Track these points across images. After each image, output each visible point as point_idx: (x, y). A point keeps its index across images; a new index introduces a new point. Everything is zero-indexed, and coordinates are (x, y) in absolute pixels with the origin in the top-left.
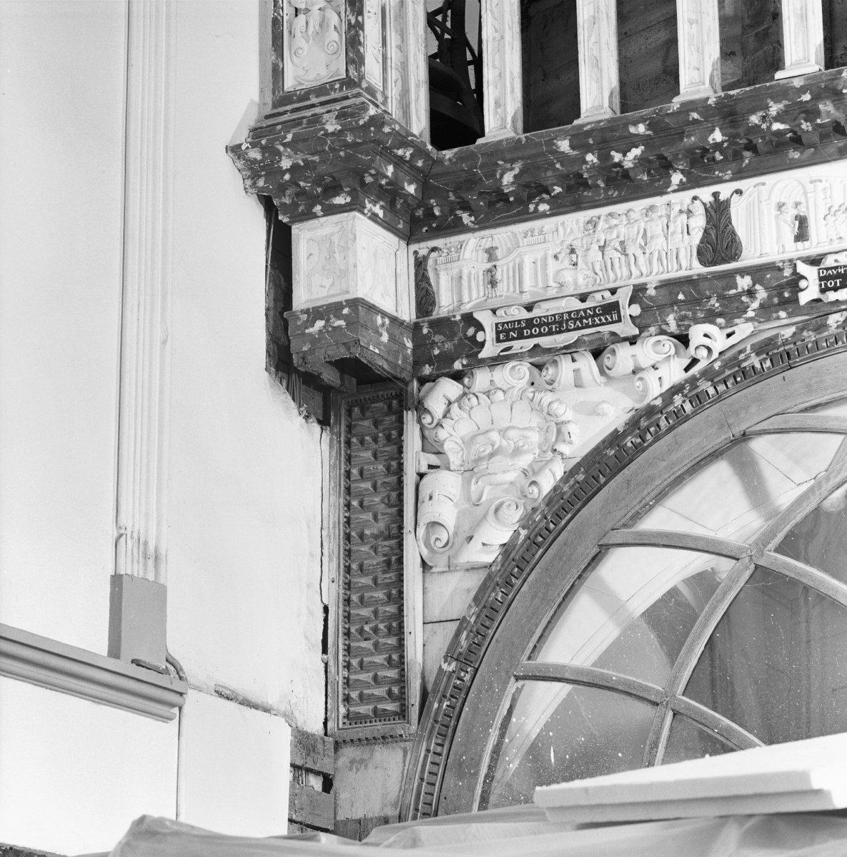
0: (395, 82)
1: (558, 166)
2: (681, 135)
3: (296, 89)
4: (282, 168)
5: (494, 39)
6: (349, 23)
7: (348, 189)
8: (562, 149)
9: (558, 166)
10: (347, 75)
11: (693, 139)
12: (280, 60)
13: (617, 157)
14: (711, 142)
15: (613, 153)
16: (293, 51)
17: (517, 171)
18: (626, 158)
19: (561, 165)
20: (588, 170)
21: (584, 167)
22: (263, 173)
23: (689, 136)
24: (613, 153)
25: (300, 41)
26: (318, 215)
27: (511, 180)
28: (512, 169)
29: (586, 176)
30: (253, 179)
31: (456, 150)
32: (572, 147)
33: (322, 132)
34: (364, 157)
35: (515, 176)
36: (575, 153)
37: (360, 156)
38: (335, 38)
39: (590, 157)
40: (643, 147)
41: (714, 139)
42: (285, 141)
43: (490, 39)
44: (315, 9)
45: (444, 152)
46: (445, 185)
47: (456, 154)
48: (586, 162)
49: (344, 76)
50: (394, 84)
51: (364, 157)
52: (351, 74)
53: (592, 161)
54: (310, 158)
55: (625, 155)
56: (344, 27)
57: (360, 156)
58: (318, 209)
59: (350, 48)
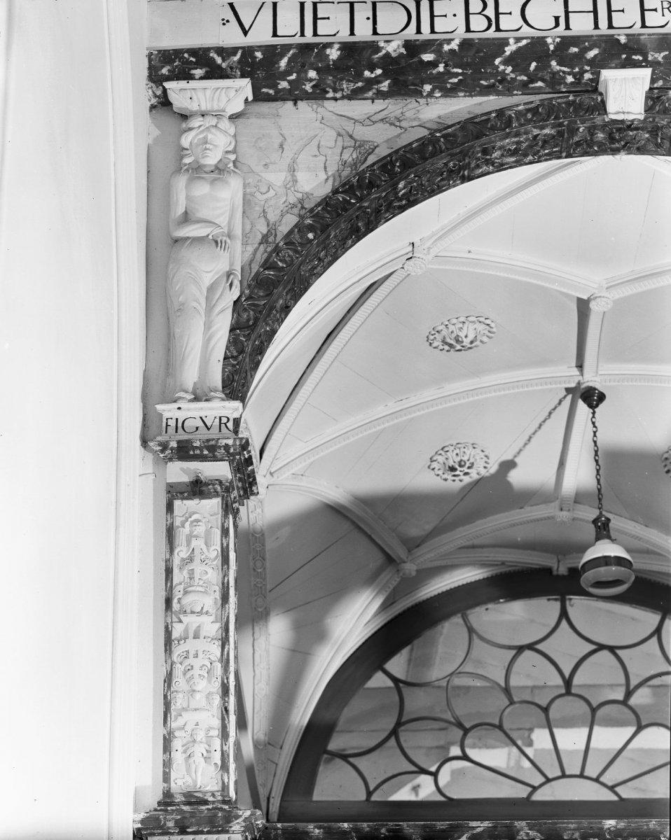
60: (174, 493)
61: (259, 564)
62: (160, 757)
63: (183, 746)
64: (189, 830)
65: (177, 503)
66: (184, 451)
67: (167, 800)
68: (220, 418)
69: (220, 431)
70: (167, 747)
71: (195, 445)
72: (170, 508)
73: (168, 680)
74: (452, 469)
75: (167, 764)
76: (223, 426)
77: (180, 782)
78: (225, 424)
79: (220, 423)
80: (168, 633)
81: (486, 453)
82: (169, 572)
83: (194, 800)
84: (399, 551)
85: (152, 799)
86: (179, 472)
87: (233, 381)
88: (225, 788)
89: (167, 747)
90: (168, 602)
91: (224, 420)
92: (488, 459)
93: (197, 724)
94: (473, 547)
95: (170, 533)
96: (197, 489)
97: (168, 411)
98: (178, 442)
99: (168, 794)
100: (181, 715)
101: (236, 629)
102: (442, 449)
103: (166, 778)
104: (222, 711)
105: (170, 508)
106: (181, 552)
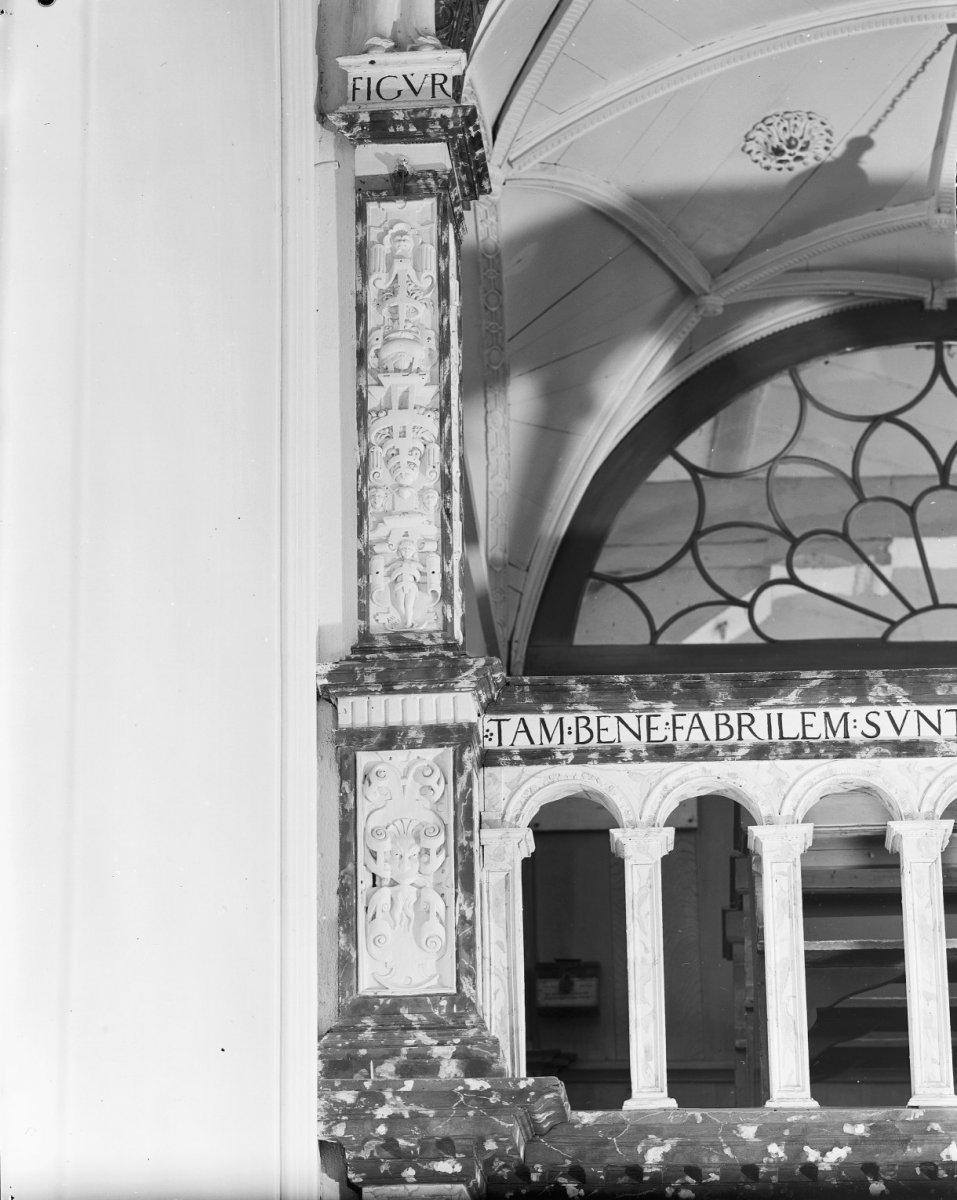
0: (495, 994)
1: (727, 1151)
2: (905, 1142)
3: (379, 994)
4: (375, 1116)
5: (643, 961)
6: (463, 917)
7: (462, 1156)
8: (743, 1136)
9: (727, 1151)
10: (458, 990)
11: (919, 1150)
12: (353, 949)
13: (812, 1155)
14: (945, 1159)
15: (806, 1148)
16: (372, 937)
17: (667, 1148)
18: (825, 1159)
19: (733, 1152)
20: (768, 1165)
21: (765, 1160)
22: (344, 1118)
23: (915, 1145)
24: (806, 1148)
25: (382, 925)
26: (408, 1180)
27: (659, 1159)
28: (661, 1145)
29: (763, 1169)
30: (327, 1122)
31: (599, 1113)
32: (757, 1135)
33: (461, 1088)
34: (502, 1123)
35: (665, 1155)
36: (757, 1140)
37: (497, 1120)
38: (441, 935)
39: (773, 1148)
40: (850, 1149)
41: (948, 1156)
42: (402, 1090)
43: (639, 961)
44: (406, 883)
45: (580, 1114)
46: (560, 1148)
47: (598, 1119)
48: (769, 1155)
49: (454, 991)
50: (493, 996)
51: (502, 1123)
52: (465, 990)
53: (777, 1154)
54: (422, 1110)
55: (823, 1154)
56: (454, 920)
57: (497, 1120)
58: (410, 1173)
59: (463, 952)
60: (368, 191)
61: (493, 299)
62: (354, 582)
63: (386, 566)
64: (396, 687)
65: (371, 207)
66: (380, 128)
67: (365, 645)
68: (433, 76)
69: (433, 96)
70: (363, 569)
71: (396, 118)
72: (361, 214)
73: (364, 470)
74: (778, 151)
75: (364, 593)
76: (438, 87)
77: (384, 618)
78: (441, 85)
79: (434, 84)
80: (362, 401)
81: (828, 127)
82: (361, 310)
83: (402, 644)
84: (698, 278)
85: (342, 645)
86: (374, 159)
87: (452, 18)
88: (447, 626)
89: (363, 569)
90: (361, 355)
91: (439, 79)
92: (831, 135)
93: (406, 535)
94: (807, 269)
95: (362, 251)
96: (401, 185)
97: (355, 66)
98: (372, 114)
99: (365, 636)
100: (382, 522)
101: (461, 394)
102: (763, 121)
103: (363, 613)
104: (442, 517)
105: (361, 214)
106: (379, 281)
